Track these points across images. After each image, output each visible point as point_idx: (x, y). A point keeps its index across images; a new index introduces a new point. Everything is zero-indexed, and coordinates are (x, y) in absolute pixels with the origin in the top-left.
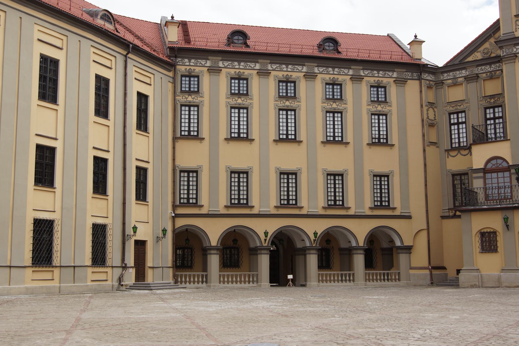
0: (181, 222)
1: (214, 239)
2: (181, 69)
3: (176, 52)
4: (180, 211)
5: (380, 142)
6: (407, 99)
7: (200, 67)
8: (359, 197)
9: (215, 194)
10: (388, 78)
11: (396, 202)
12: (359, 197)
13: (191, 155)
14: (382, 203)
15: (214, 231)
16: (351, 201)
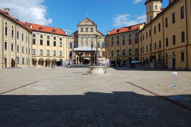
0: (33, 57)
1: (38, 60)
2: (33, 33)
3: (32, 30)
4: (33, 56)
5: (61, 46)
6: (64, 39)
7: (35, 33)
8: (58, 54)
9: (38, 53)
10: (62, 37)
11: (62, 55)
12: (58, 54)
13: (34, 47)
14: (61, 55)
15: (38, 59)
16: (57, 55)
